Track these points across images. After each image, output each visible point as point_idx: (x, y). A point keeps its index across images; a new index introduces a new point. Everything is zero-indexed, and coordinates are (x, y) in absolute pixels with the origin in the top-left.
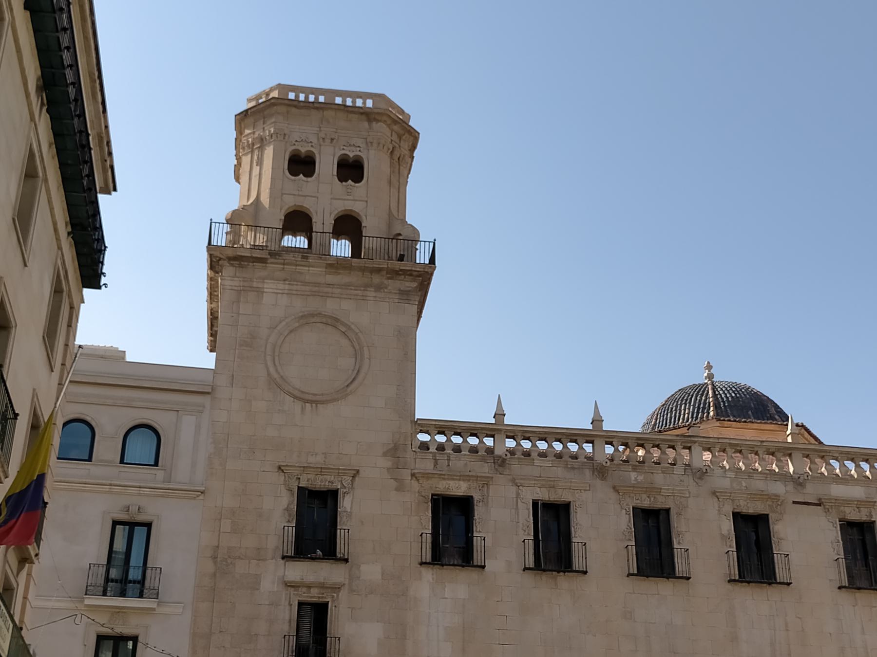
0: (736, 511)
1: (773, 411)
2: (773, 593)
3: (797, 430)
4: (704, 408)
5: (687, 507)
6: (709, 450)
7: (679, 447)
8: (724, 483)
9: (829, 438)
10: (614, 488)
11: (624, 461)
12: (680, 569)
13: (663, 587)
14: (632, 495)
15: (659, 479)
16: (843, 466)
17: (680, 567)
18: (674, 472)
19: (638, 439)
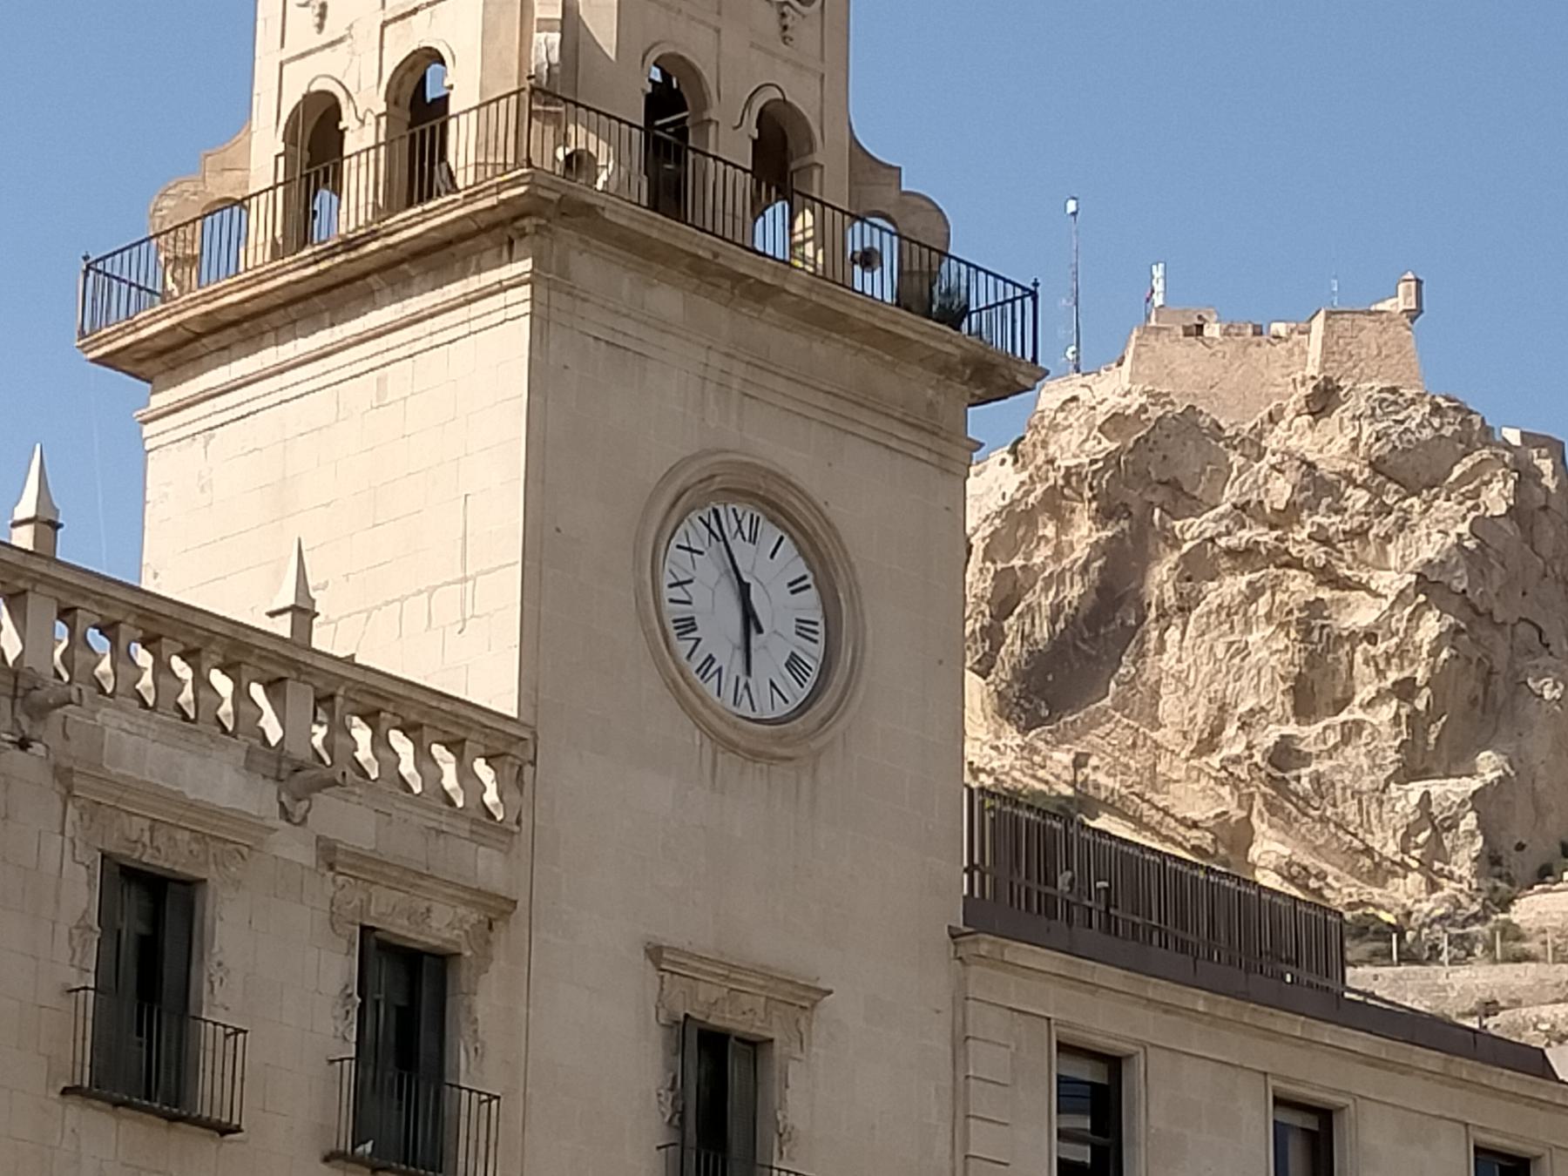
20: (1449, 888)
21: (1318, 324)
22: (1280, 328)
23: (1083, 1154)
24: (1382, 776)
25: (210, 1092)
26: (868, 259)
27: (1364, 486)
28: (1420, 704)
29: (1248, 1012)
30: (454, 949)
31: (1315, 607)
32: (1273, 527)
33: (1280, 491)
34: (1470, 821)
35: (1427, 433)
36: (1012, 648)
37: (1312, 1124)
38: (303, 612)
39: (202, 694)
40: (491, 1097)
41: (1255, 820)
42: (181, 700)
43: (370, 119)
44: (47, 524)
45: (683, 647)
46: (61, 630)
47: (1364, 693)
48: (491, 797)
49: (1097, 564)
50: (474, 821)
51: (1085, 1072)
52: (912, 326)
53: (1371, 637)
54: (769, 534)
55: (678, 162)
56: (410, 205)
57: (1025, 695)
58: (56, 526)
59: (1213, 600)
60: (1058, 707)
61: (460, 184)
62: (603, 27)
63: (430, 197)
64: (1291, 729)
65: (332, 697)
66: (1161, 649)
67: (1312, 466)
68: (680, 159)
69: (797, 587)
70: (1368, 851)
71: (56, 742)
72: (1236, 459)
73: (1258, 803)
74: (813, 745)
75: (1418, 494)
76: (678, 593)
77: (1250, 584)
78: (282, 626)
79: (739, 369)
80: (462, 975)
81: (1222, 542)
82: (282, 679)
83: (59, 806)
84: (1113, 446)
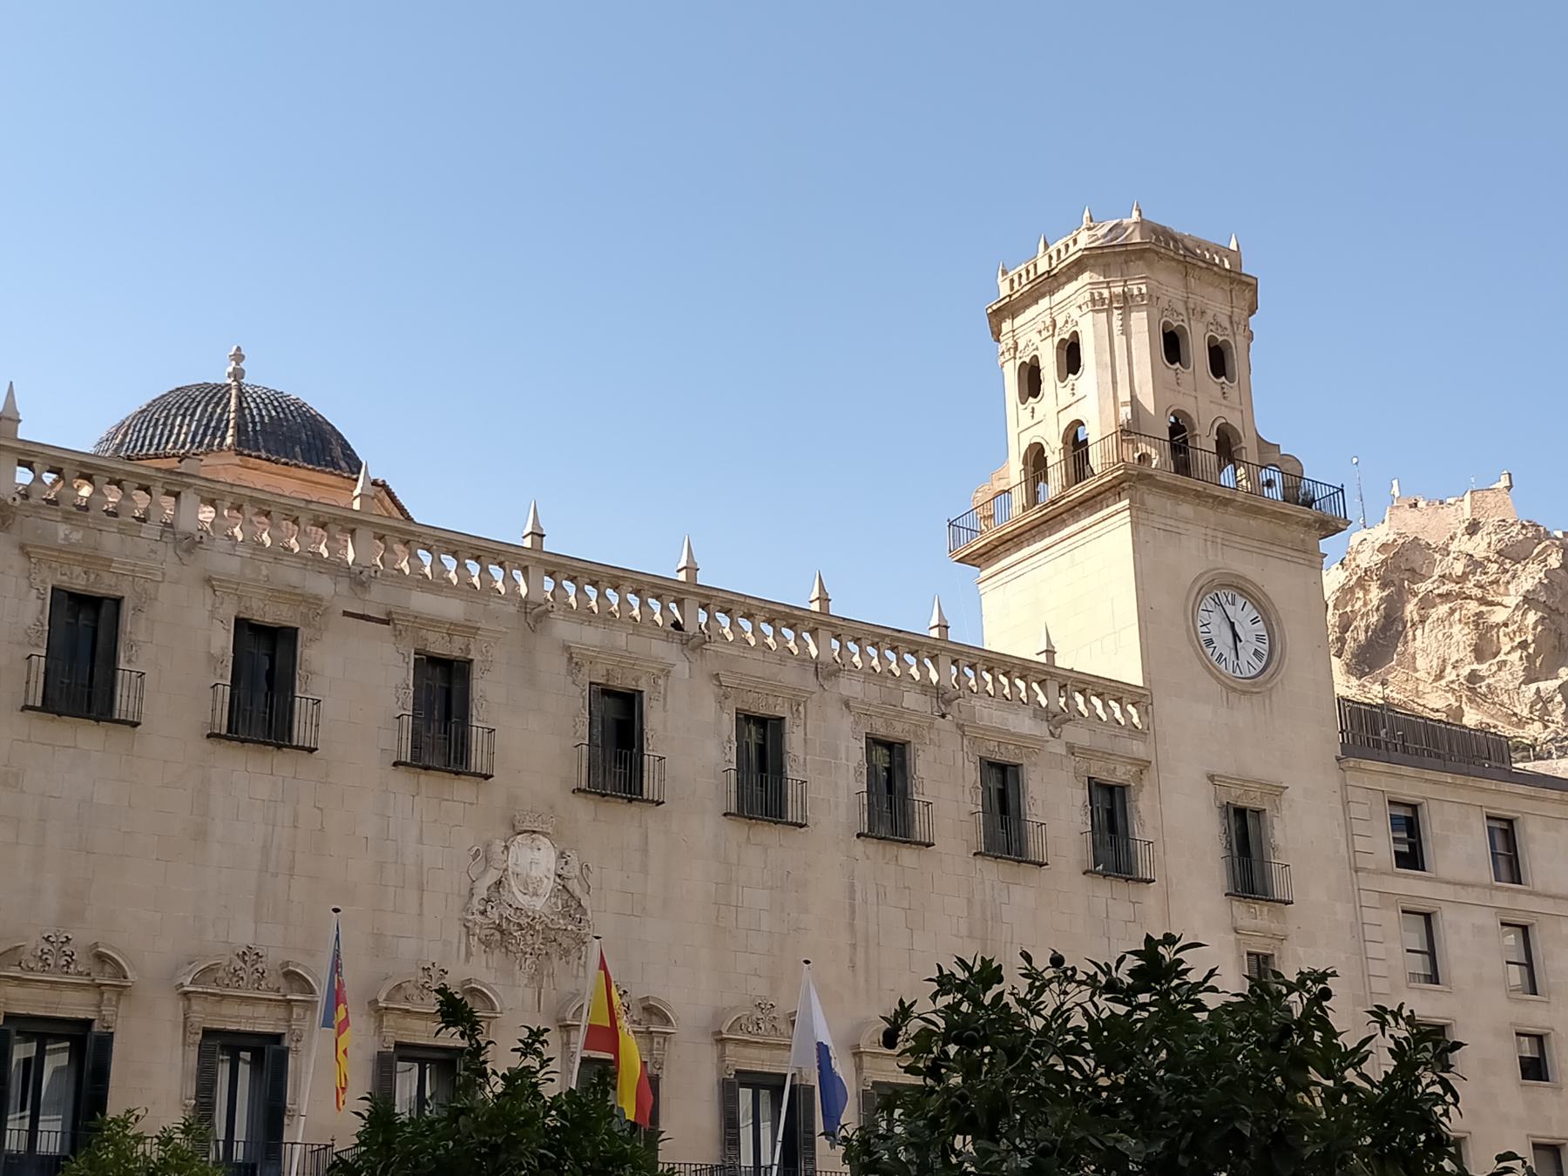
0: (241, 616)
1: (338, 451)
2: (283, 762)
3: (372, 491)
4: (217, 428)
5: (156, 599)
6: (212, 503)
7: (157, 489)
8: (232, 566)
9: (423, 513)
10: (22, 547)
11: (49, 501)
12: (124, 707)
13: (87, 736)
14: (54, 565)
15: (111, 542)
16: (437, 561)
17: (123, 704)
18: (142, 535)
19: (82, 464)
20: (1553, 727)
21: (1468, 497)
22: (1451, 500)
23: (1405, 848)
24: (1517, 683)
25: (1034, 849)
26: (1270, 484)
27: (1495, 562)
28: (1531, 651)
30: (1126, 783)
31: (1480, 615)
32: (1457, 583)
33: (1459, 568)
34: (1559, 698)
35: (1521, 537)
36: (1350, 645)
37: (1504, 825)
40: (1150, 843)
41: (1463, 706)
42: (1005, 692)
44: (943, 627)
46: (954, 669)
47: (1505, 648)
49: (1382, 607)
50: (1129, 730)
51: (1402, 812)
52: (1291, 509)
53: (1506, 625)
55: (1185, 453)
56: (1077, 483)
57: (1358, 663)
58: (947, 627)
59: (1435, 617)
60: (1372, 668)
61: (1096, 472)
62: (1148, 401)
63: (1084, 479)
64: (1476, 666)
65: (1066, 685)
66: (1414, 639)
67: (1471, 556)
68: (1186, 452)
70: (1515, 714)
71: (956, 715)
72: (1438, 556)
73: (1464, 699)
75: (1519, 562)
76: (1205, 630)
77: (1450, 608)
78: (1043, 659)
79: (1220, 535)
80: (1132, 793)
81: (1436, 592)
82: (1045, 680)
83: (960, 740)
84: (1384, 557)
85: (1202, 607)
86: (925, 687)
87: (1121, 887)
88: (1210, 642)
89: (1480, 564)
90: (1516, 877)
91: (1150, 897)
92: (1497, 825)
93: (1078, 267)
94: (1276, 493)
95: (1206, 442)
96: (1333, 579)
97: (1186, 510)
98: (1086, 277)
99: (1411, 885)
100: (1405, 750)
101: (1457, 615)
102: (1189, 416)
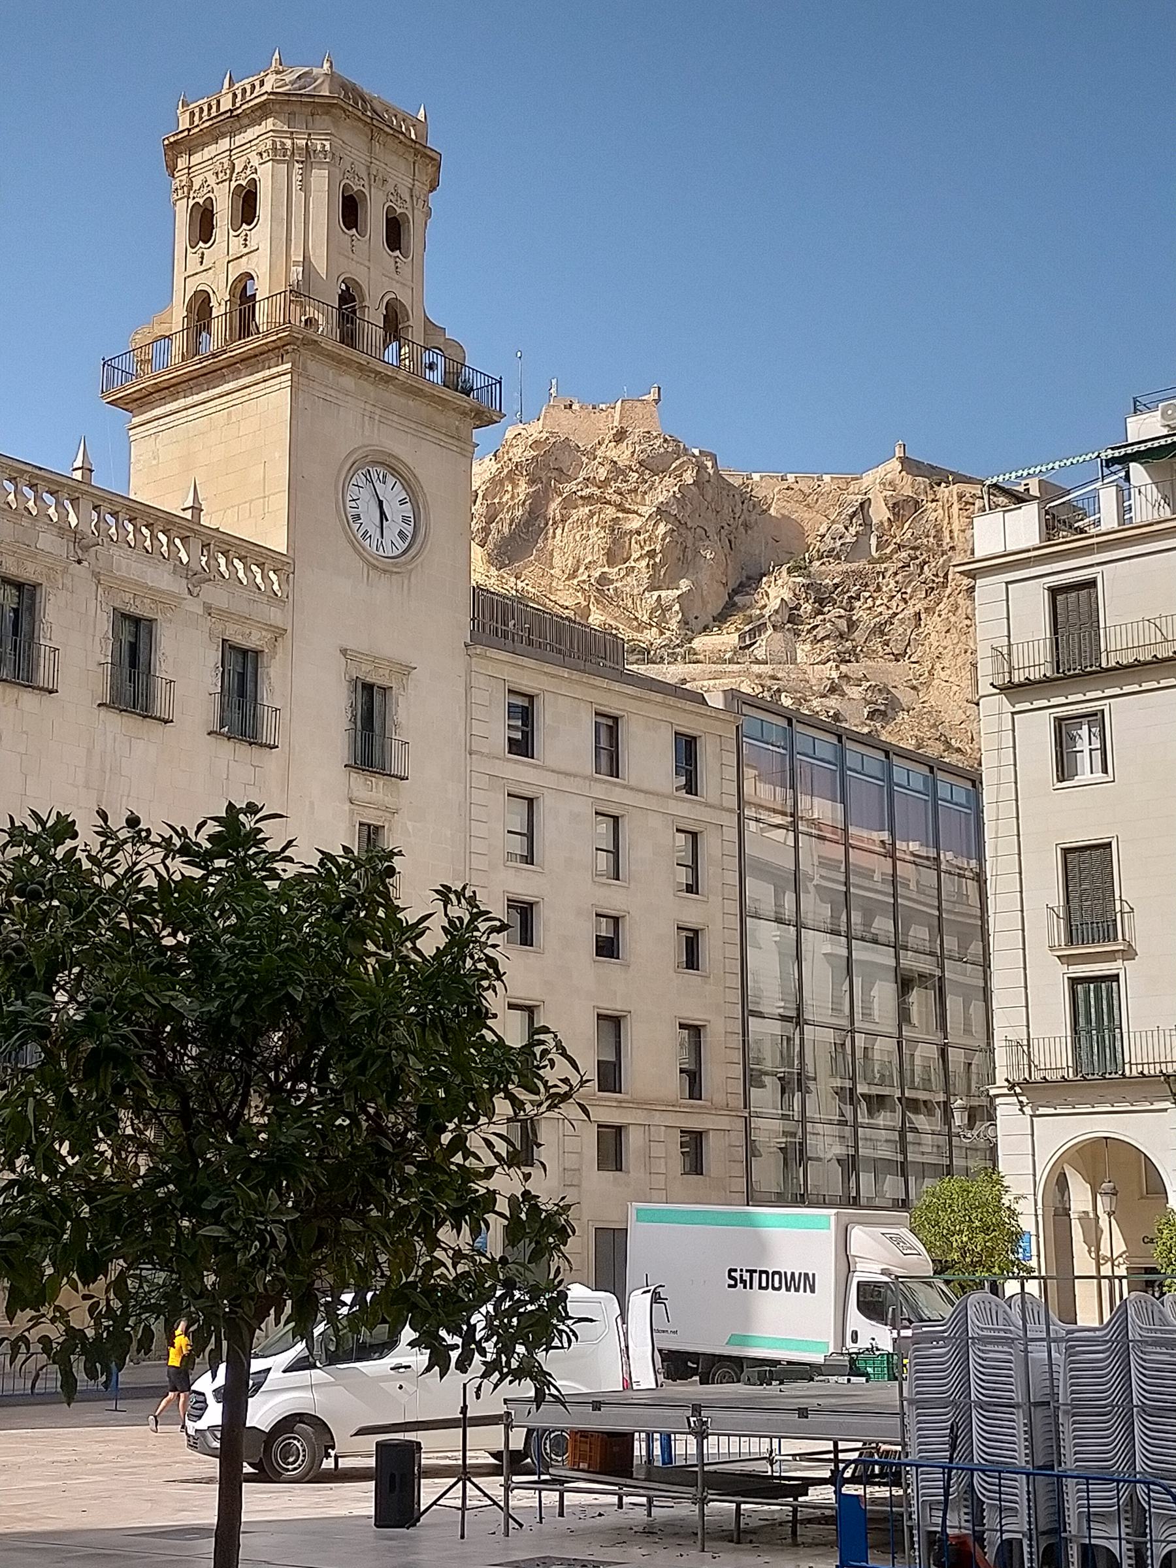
22: (603, 406)
23: (518, 736)
24: (642, 589)
27: (636, 471)
28: (658, 560)
29: (585, 678)
32: (599, 488)
33: (602, 473)
34: (677, 607)
35: (662, 450)
36: (494, 536)
38: (196, 509)
39: (154, 542)
40: (276, 709)
41: (591, 606)
42: (146, 544)
43: (223, 303)
44: (87, 470)
45: (355, 526)
46: (95, 515)
47: (635, 556)
48: (276, 587)
49: (528, 502)
50: (269, 597)
51: (519, 701)
54: (391, 480)
55: (352, 324)
56: (240, 339)
58: (91, 471)
61: (261, 331)
63: (248, 336)
64: (606, 569)
65: (209, 544)
66: (554, 537)
67: (615, 463)
69: (402, 502)
70: (636, 618)
71: (93, 561)
73: (592, 599)
74: (409, 567)
75: (657, 475)
77: (590, 510)
78: (188, 515)
79: (378, 411)
80: (264, 660)
81: (579, 493)
82: (188, 537)
83: (95, 587)
84: (535, 454)
85: (354, 481)
86: (63, 529)
87: (243, 749)
88: (358, 517)
89: (623, 472)
90: (614, 771)
91: (271, 761)
92: (601, 720)
93: (262, 111)
94: (436, 376)
95: (374, 316)
96: (483, 470)
97: (348, 381)
98: (269, 123)
99: (520, 772)
100: (530, 643)
101: (595, 518)
102: (360, 286)
